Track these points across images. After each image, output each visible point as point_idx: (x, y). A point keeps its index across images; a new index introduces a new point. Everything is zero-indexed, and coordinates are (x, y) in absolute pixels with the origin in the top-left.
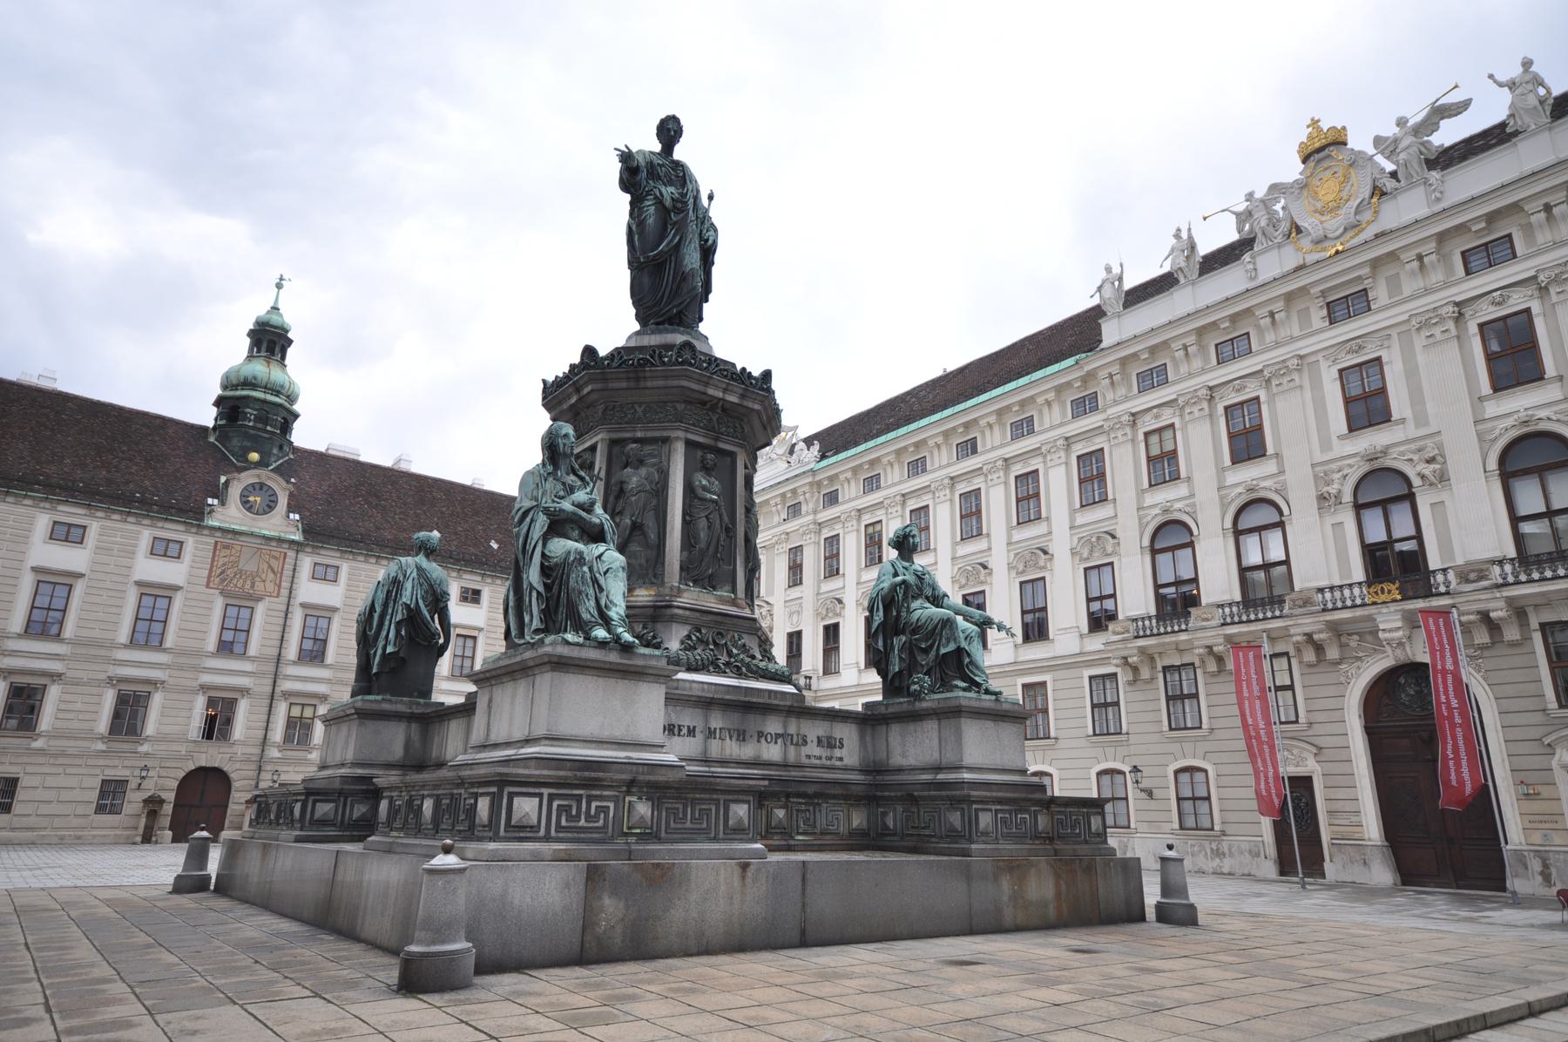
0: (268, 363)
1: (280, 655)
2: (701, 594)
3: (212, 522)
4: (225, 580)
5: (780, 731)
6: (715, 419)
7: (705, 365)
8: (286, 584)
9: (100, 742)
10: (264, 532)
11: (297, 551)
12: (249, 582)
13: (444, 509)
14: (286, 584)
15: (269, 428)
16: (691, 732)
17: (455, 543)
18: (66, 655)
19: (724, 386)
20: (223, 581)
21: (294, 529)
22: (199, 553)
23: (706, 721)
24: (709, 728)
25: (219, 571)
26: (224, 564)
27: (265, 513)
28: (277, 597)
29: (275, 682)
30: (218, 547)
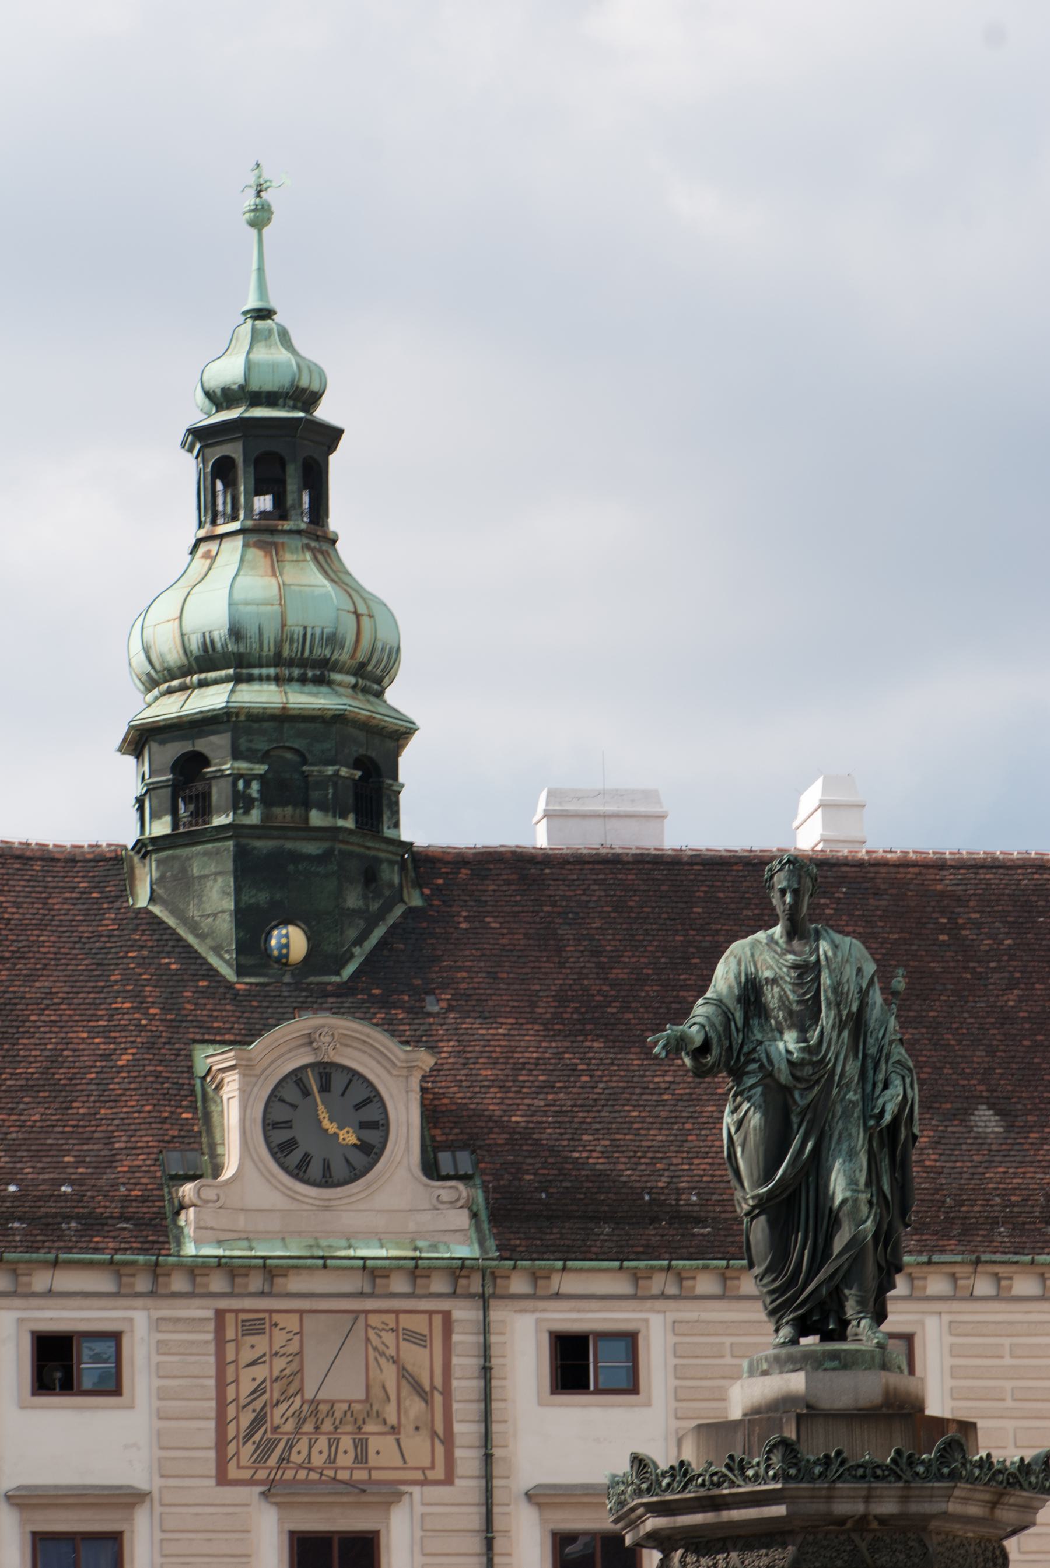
4: (272, 1445)
6: (863, 1546)
7: (818, 1470)
8: (466, 1430)
11: (484, 1301)
12: (346, 1442)
13: (1011, 999)
14: (466, 1430)
15: (317, 818)
19: (864, 1493)
20: (264, 1450)
21: (462, 1219)
26: (258, 1391)
27: (355, 1174)
28: (449, 1480)
30: (230, 1334)
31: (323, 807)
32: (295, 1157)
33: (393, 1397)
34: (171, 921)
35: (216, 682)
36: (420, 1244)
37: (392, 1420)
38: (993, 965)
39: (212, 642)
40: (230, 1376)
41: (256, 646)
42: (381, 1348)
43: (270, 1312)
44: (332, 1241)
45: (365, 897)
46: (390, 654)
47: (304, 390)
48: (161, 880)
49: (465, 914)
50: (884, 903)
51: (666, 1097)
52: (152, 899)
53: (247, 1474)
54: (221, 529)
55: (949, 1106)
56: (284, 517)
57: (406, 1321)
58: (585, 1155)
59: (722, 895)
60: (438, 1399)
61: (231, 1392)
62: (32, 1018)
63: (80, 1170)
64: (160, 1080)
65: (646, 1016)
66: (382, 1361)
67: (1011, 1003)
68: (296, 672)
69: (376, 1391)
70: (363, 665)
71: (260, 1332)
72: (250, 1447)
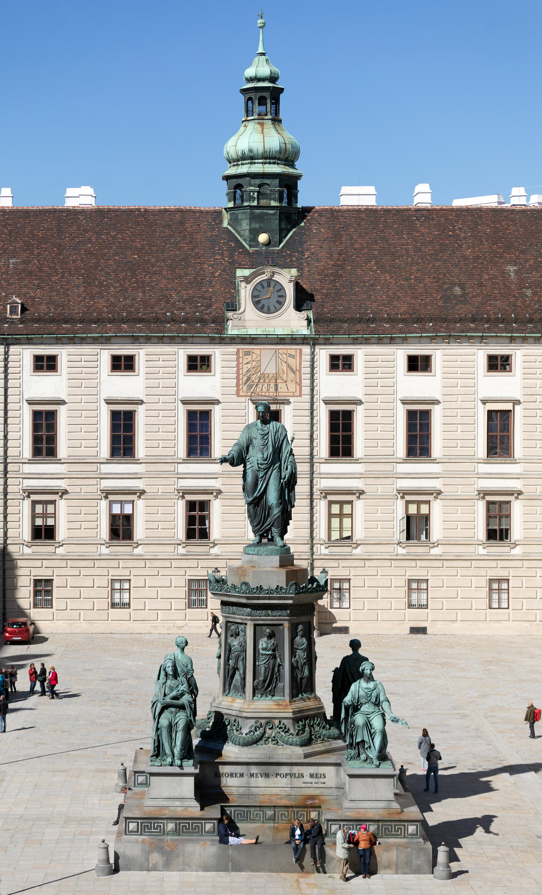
0: (262, 125)
1: (312, 454)
2: (265, 703)
3: (232, 330)
5: (288, 772)
7: (255, 591)
8: (306, 382)
9: (180, 547)
10: (280, 331)
12: (272, 385)
15: (273, 203)
16: (242, 775)
17: (479, 299)
18: (142, 474)
20: (250, 387)
21: (305, 323)
22: (226, 364)
23: (248, 770)
24: (250, 774)
25: (245, 379)
26: (248, 371)
28: (300, 395)
29: (312, 482)
30: (241, 355)
31: (275, 200)
32: (260, 305)
33: (285, 373)
34: (233, 231)
35: (246, 164)
36: (294, 330)
37: (285, 379)
38: (464, 241)
39: (244, 153)
40: (241, 367)
41: (256, 154)
42: (282, 359)
43: (252, 349)
44: (270, 329)
45: (287, 224)
46: (295, 154)
47: (273, 77)
48: (230, 220)
49: (315, 228)
50: (434, 222)
51: (366, 284)
52: (229, 224)
53: (245, 394)
54: (249, 118)
55: (447, 286)
56: (266, 115)
57: (289, 352)
58: (342, 302)
59: (388, 221)
60: (298, 373)
61: (241, 371)
62: (193, 261)
63: (202, 308)
64: (226, 280)
65: (363, 259)
66: (282, 362)
67: (468, 254)
68: (268, 161)
69: (281, 371)
70: (287, 158)
71: (249, 355)
72: (246, 386)
